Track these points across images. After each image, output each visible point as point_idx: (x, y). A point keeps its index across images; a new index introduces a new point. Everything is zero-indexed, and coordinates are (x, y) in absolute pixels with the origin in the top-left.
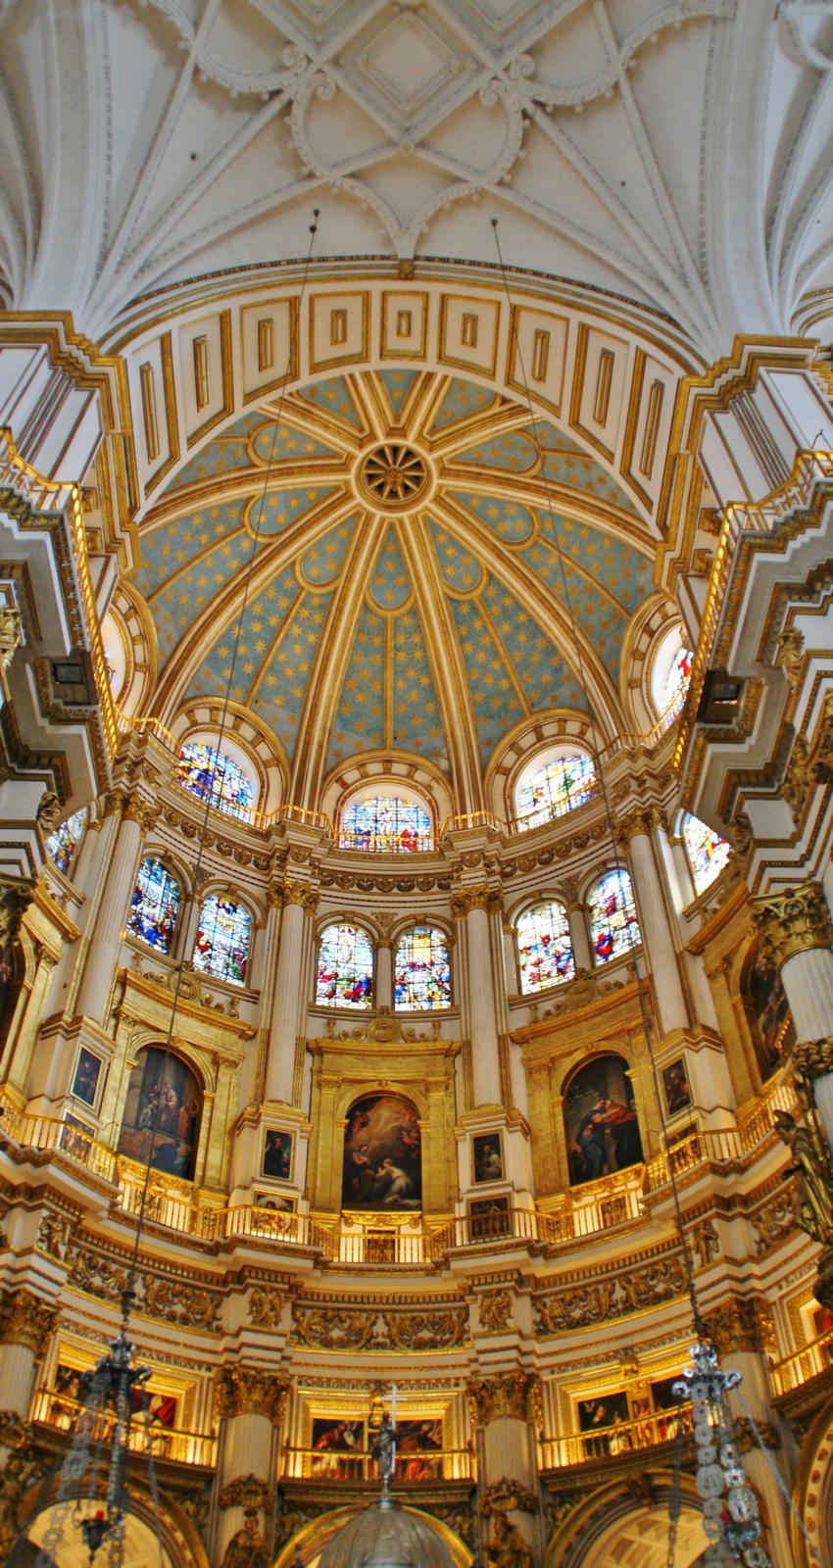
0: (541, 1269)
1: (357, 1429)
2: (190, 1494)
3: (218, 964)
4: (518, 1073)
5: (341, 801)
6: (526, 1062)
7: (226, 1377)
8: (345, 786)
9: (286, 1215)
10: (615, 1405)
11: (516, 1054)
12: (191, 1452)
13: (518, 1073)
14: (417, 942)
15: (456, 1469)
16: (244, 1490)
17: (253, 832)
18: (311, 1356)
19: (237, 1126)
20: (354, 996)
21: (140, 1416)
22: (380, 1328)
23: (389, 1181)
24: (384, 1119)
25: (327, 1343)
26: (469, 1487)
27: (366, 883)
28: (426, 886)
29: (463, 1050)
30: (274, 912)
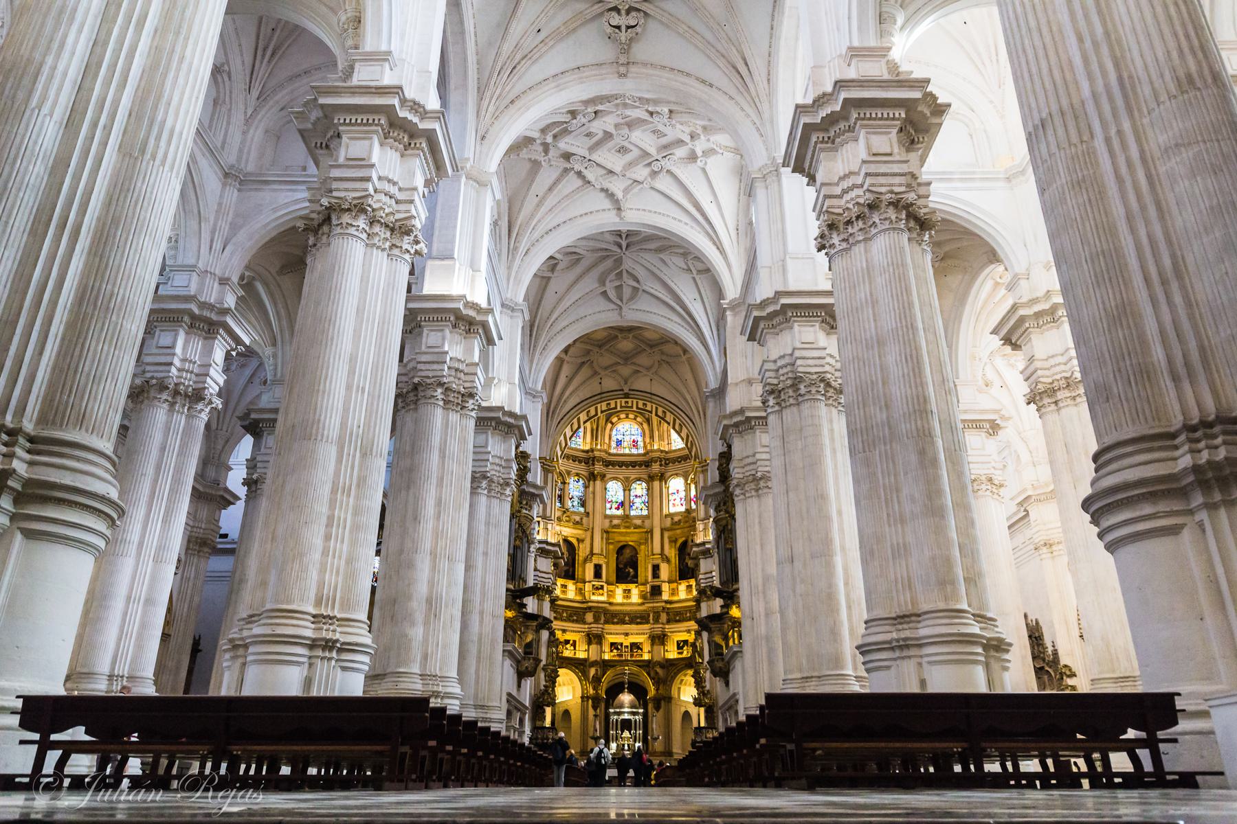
0: (668, 606)
1: (621, 644)
2: (582, 664)
3: (575, 503)
4: (666, 541)
5: (611, 430)
6: (669, 538)
7: (588, 635)
8: (612, 424)
9: (601, 591)
10: (686, 642)
11: (666, 535)
12: (581, 655)
13: (666, 541)
14: (638, 487)
15: (646, 657)
16: (594, 664)
17: (583, 451)
18: (610, 627)
19: (585, 561)
20: (618, 508)
21: (568, 646)
22: (627, 618)
23: (629, 572)
24: (627, 553)
25: (613, 623)
26: (649, 662)
27: (621, 464)
28: (640, 465)
29: (651, 532)
30: (591, 483)
